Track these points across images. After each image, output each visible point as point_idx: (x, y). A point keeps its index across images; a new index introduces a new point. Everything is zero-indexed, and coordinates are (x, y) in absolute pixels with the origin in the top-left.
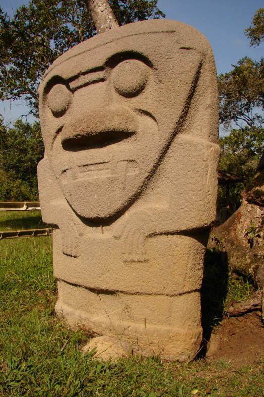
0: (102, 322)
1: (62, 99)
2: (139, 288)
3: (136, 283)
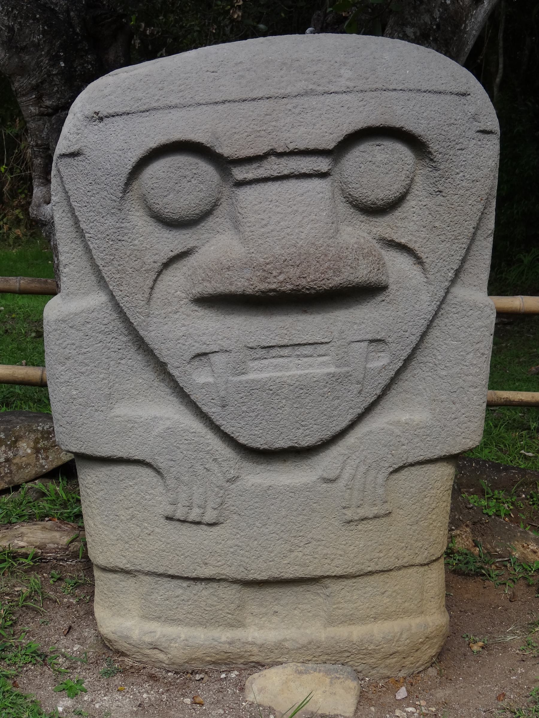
0: (285, 640)
1: (201, 195)
2: (372, 564)
3: (368, 556)
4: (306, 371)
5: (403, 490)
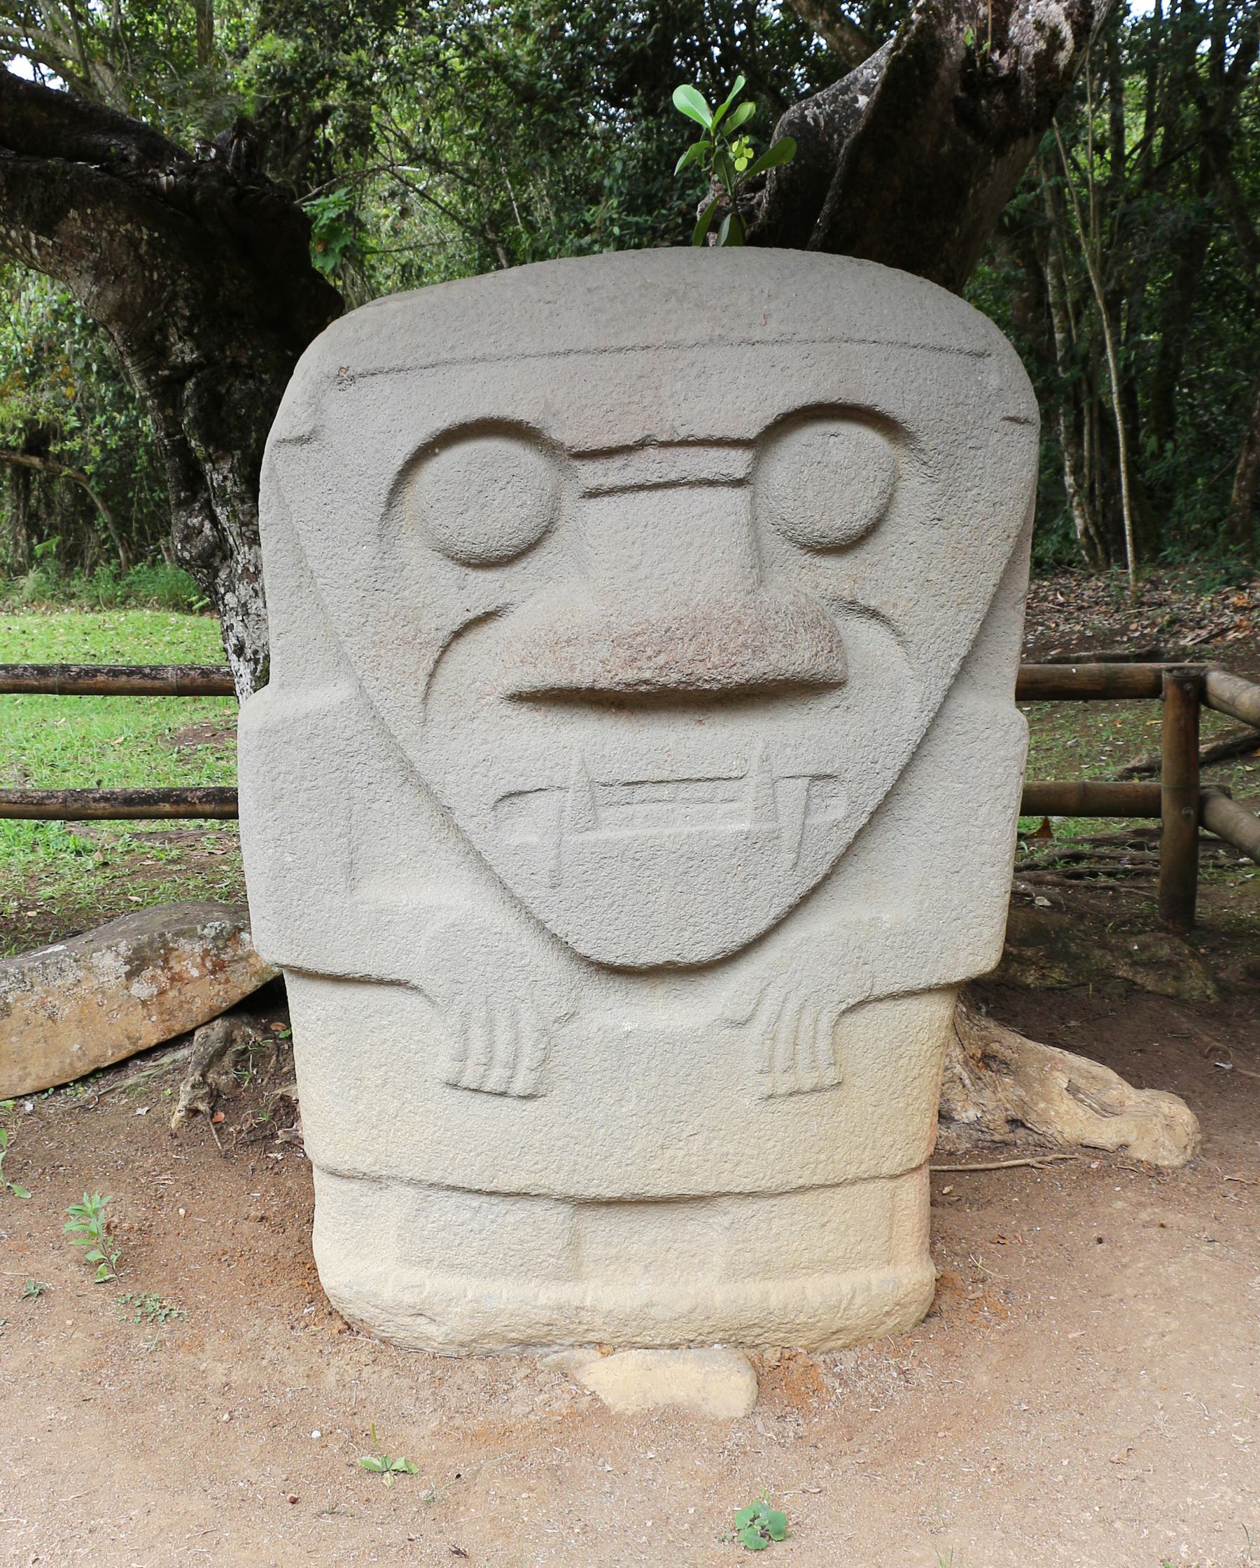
1: (524, 512)
4: (699, 828)
5: (862, 1044)
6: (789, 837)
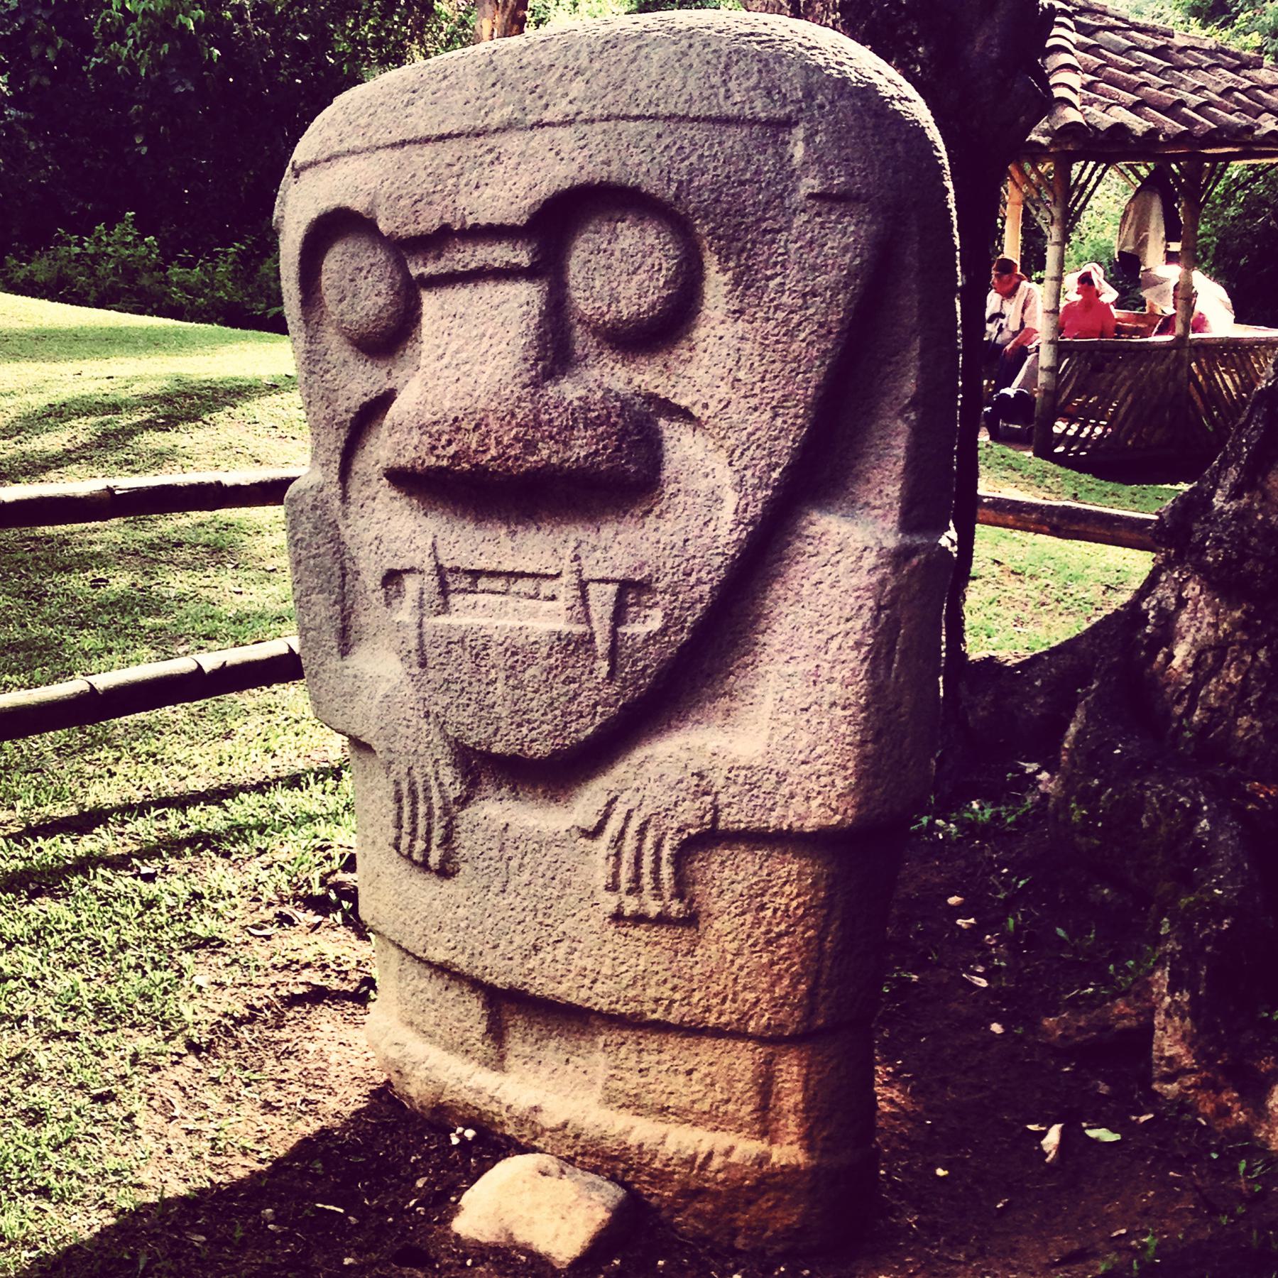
1: (381, 301)
6: (602, 645)
